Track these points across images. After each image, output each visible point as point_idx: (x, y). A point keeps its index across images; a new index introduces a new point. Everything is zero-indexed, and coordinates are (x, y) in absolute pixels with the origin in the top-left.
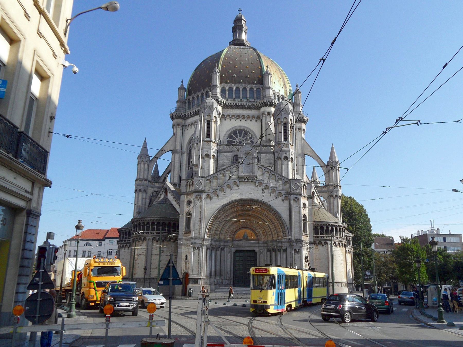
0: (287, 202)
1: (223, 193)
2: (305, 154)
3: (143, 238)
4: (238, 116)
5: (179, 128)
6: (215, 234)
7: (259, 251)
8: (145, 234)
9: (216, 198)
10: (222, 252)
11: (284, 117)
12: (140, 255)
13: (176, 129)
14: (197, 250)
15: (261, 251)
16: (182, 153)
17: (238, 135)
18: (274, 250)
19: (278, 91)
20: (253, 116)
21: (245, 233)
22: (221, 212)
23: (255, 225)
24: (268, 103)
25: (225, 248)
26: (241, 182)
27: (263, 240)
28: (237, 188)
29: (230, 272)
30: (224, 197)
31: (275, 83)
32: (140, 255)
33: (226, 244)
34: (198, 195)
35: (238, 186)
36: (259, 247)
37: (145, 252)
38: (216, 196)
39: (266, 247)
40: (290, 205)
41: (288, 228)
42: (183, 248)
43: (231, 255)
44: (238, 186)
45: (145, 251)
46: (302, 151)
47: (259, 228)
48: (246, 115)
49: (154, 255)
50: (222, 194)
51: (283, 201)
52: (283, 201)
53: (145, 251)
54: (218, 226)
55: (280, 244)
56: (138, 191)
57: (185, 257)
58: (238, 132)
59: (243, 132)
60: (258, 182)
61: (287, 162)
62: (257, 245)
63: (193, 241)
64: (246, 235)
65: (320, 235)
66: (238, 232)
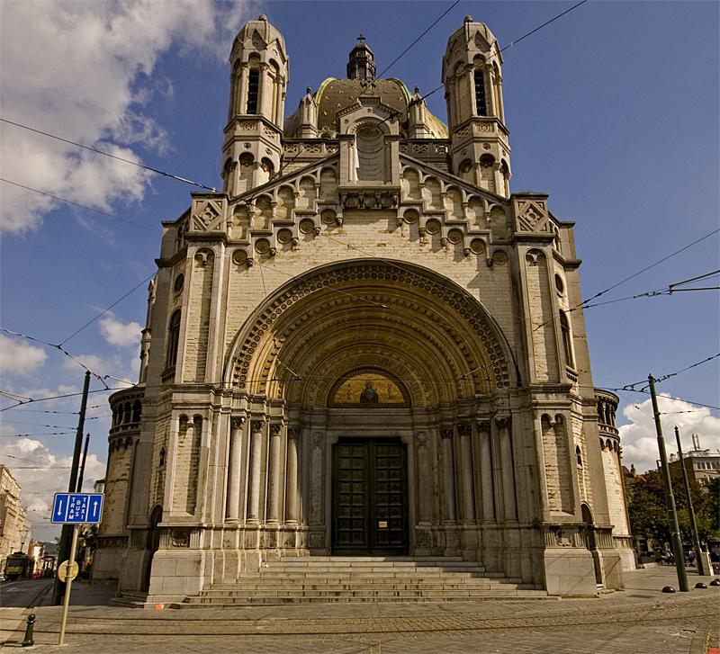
0: (502, 271)
7: (415, 437)
12: (118, 480)
14: (191, 426)
18: (464, 429)
21: (369, 385)
23: (398, 359)
25: (305, 432)
26: (349, 214)
29: (319, 508)
32: (118, 480)
33: (306, 418)
36: (412, 424)
39: (435, 423)
41: (513, 350)
42: (157, 428)
43: (324, 454)
51: (490, 264)
52: (488, 266)
55: (484, 409)
57: (159, 455)
60: (403, 209)
61: (490, 172)
62: (409, 420)
64: (369, 390)
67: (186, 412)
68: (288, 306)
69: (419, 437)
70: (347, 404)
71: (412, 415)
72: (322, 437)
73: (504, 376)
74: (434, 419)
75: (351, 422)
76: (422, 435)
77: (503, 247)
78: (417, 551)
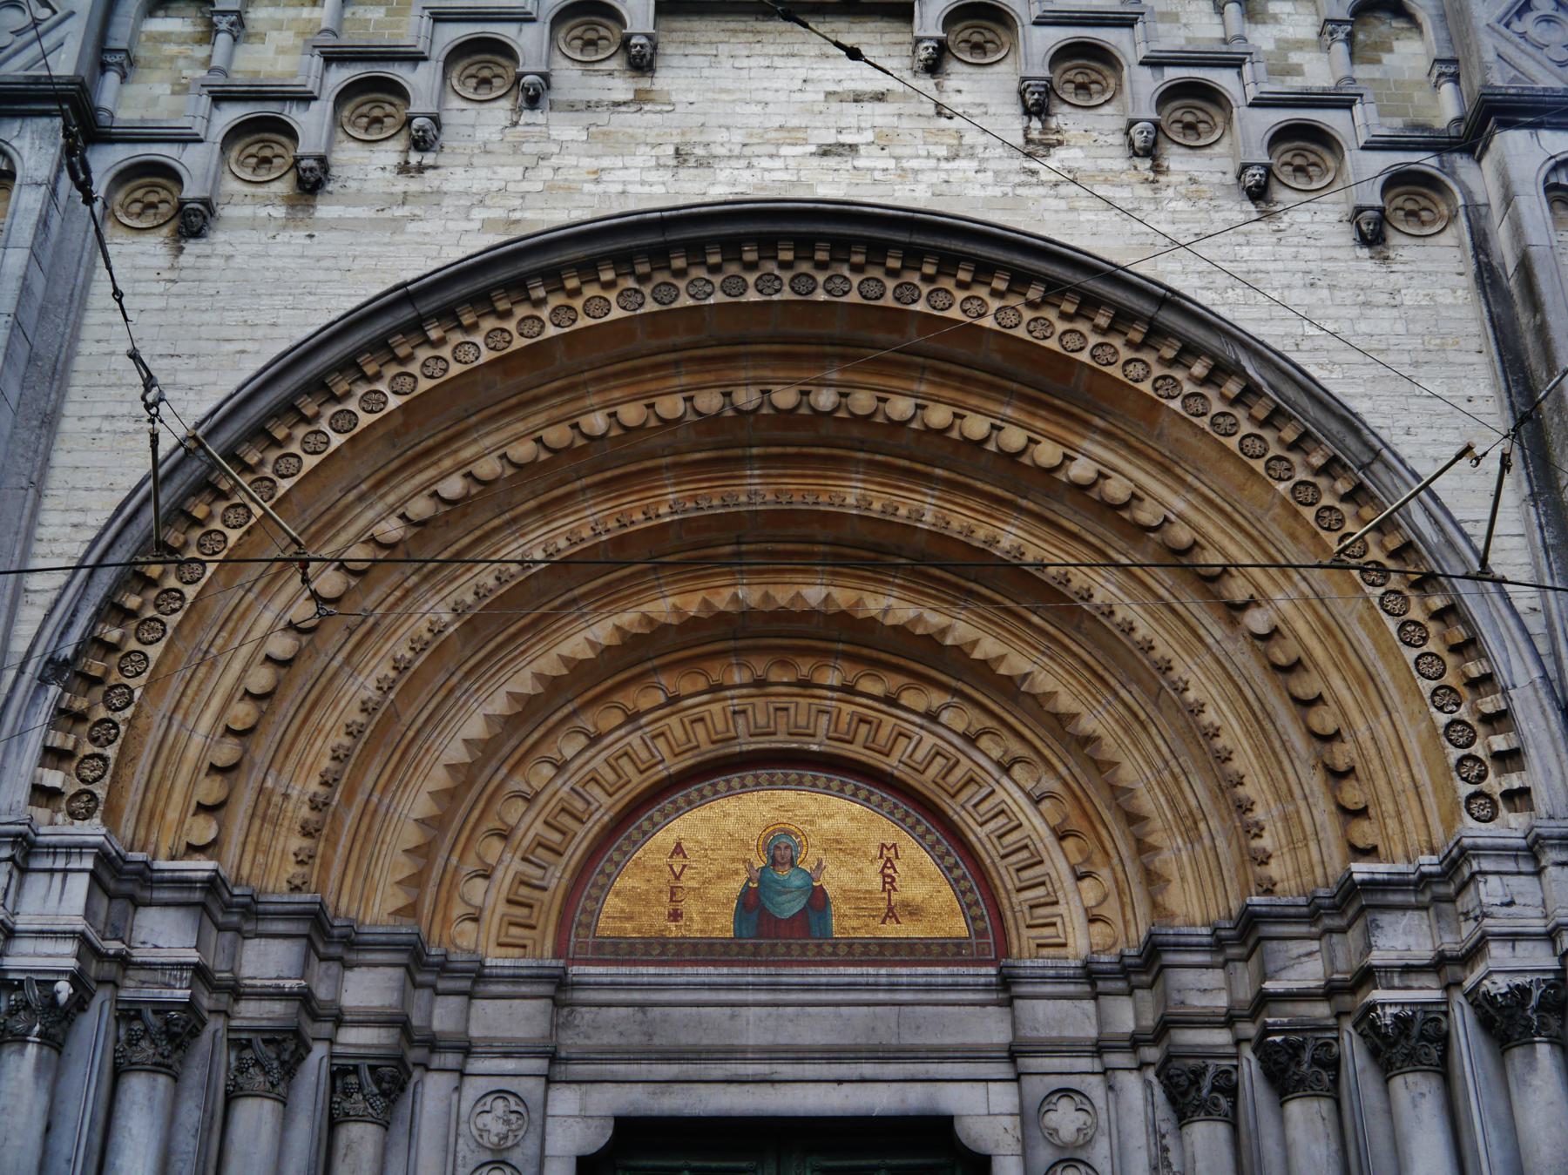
1: (390, 153)
6: (211, 790)
7: (1029, 1118)
9: (279, 212)
10: (360, 1138)
15: (1065, 1119)
22: (345, 421)
25: (433, 1091)
27: (1080, 942)
28: (622, 87)
30: (405, 198)
33: (443, 1016)
35: (642, 63)
36: (1013, 1053)
38: (284, 187)
39: (1135, 1042)
44: (642, 63)
62: (992, 1028)
64: (783, 873)
66: (665, 837)
68: (365, 419)
69: (1052, 1119)
70: (663, 942)
71: (1009, 1003)
72: (535, 1118)
73: (1498, 757)
74: (1125, 1016)
75: (686, 1039)
76: (1065, 1106)
77: (1427, 161)
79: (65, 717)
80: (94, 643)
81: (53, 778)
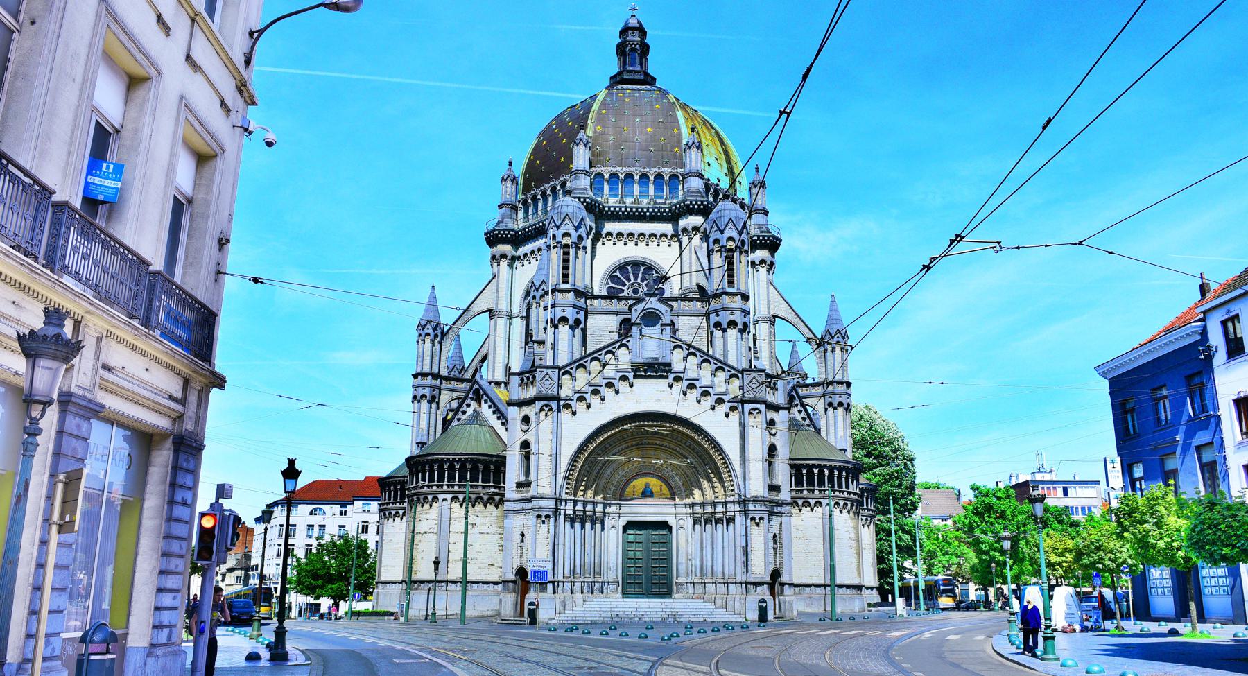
0: (735, 417)
2: (774, 316)
3: (430, 497)
4: (631, 235)
5: (506, 263)
8: (435, 488)
11: (729, 236)
12: (425, 533)
13: (498, 265)
16: (511, 317)
17: (631, 275)
19: (716, 182)
20: (664, 235)
21: (647, 485)
24: (694, 207)
31: (709, 165)
32: (425, 533)
34: (546, 406)
37: (436, 527)
38: (585, 406)
40: (742, 426)
45: (436, 524)
46: (769, 308)
47: (677, 475)
48: (647, 234)
49: (455, 533)
50: (594, 401)
51: (727, 416)
53: (436, 524)
54: (588, 471)
55: (720, 508)
56: (418, 398)
58: (630, 270)
59: (642, 268)
60: (671, 376)
63: (536, 503)
65: (805, 487)
66: (632, 484)
67: (541, 513)
74: (689, 510)
77: (736, 404)
78: (676, 596)
79: (568, 484)
80: (570, 474)
81: (567, 491)
